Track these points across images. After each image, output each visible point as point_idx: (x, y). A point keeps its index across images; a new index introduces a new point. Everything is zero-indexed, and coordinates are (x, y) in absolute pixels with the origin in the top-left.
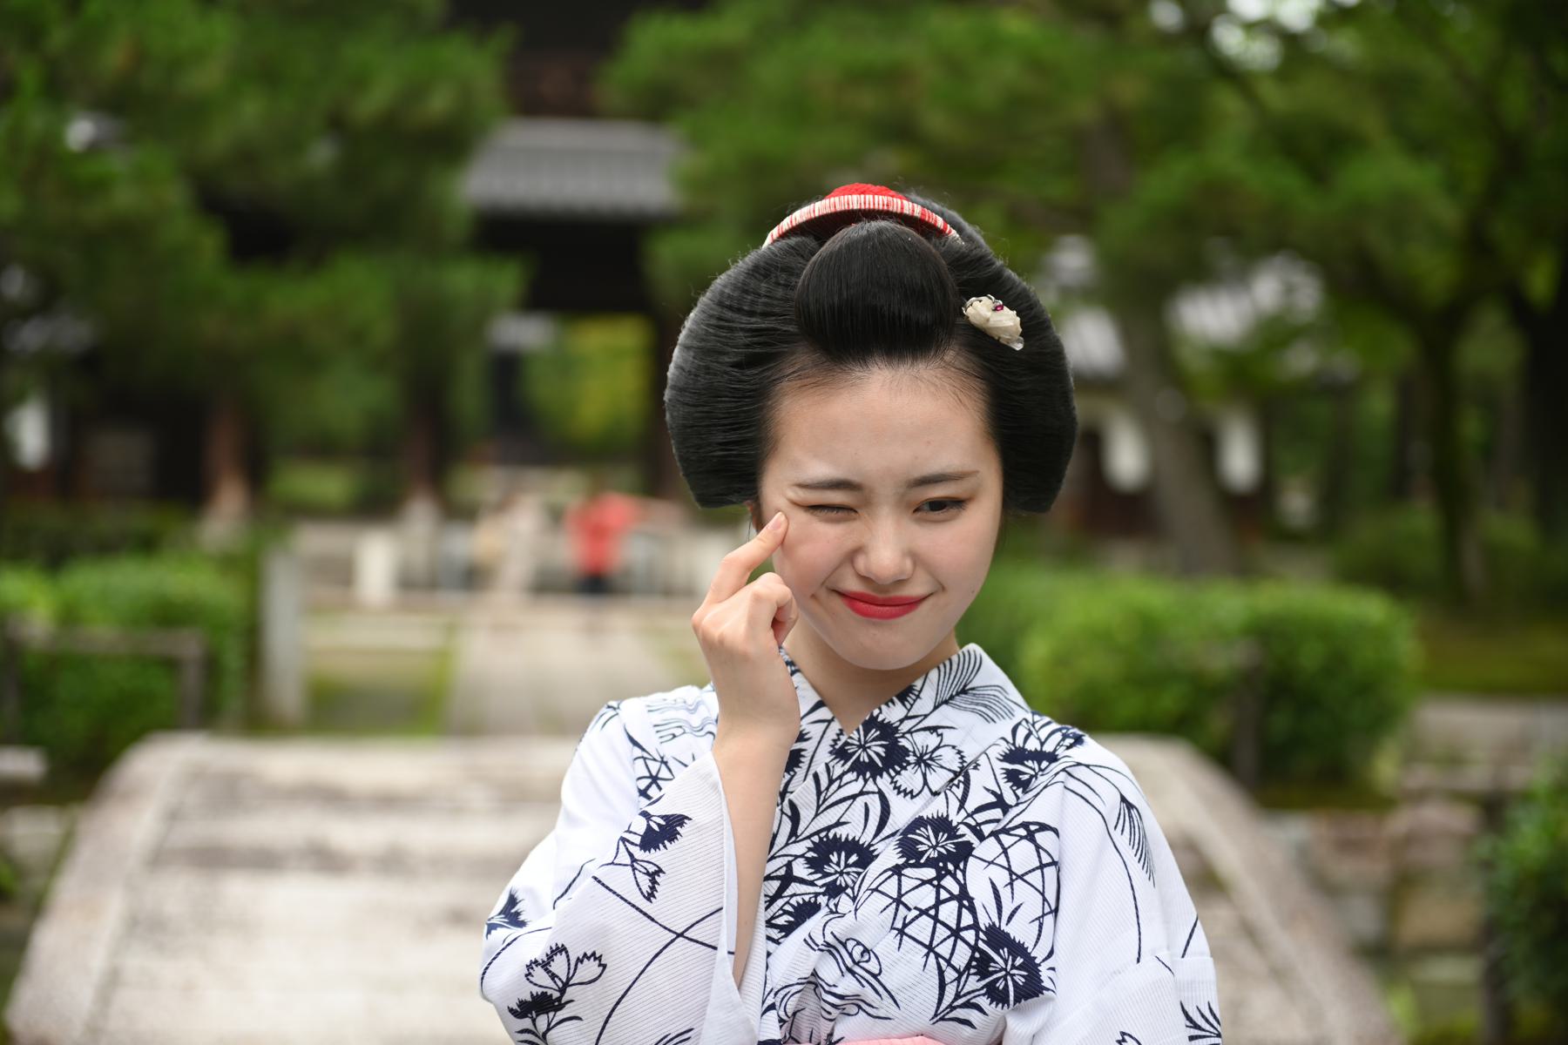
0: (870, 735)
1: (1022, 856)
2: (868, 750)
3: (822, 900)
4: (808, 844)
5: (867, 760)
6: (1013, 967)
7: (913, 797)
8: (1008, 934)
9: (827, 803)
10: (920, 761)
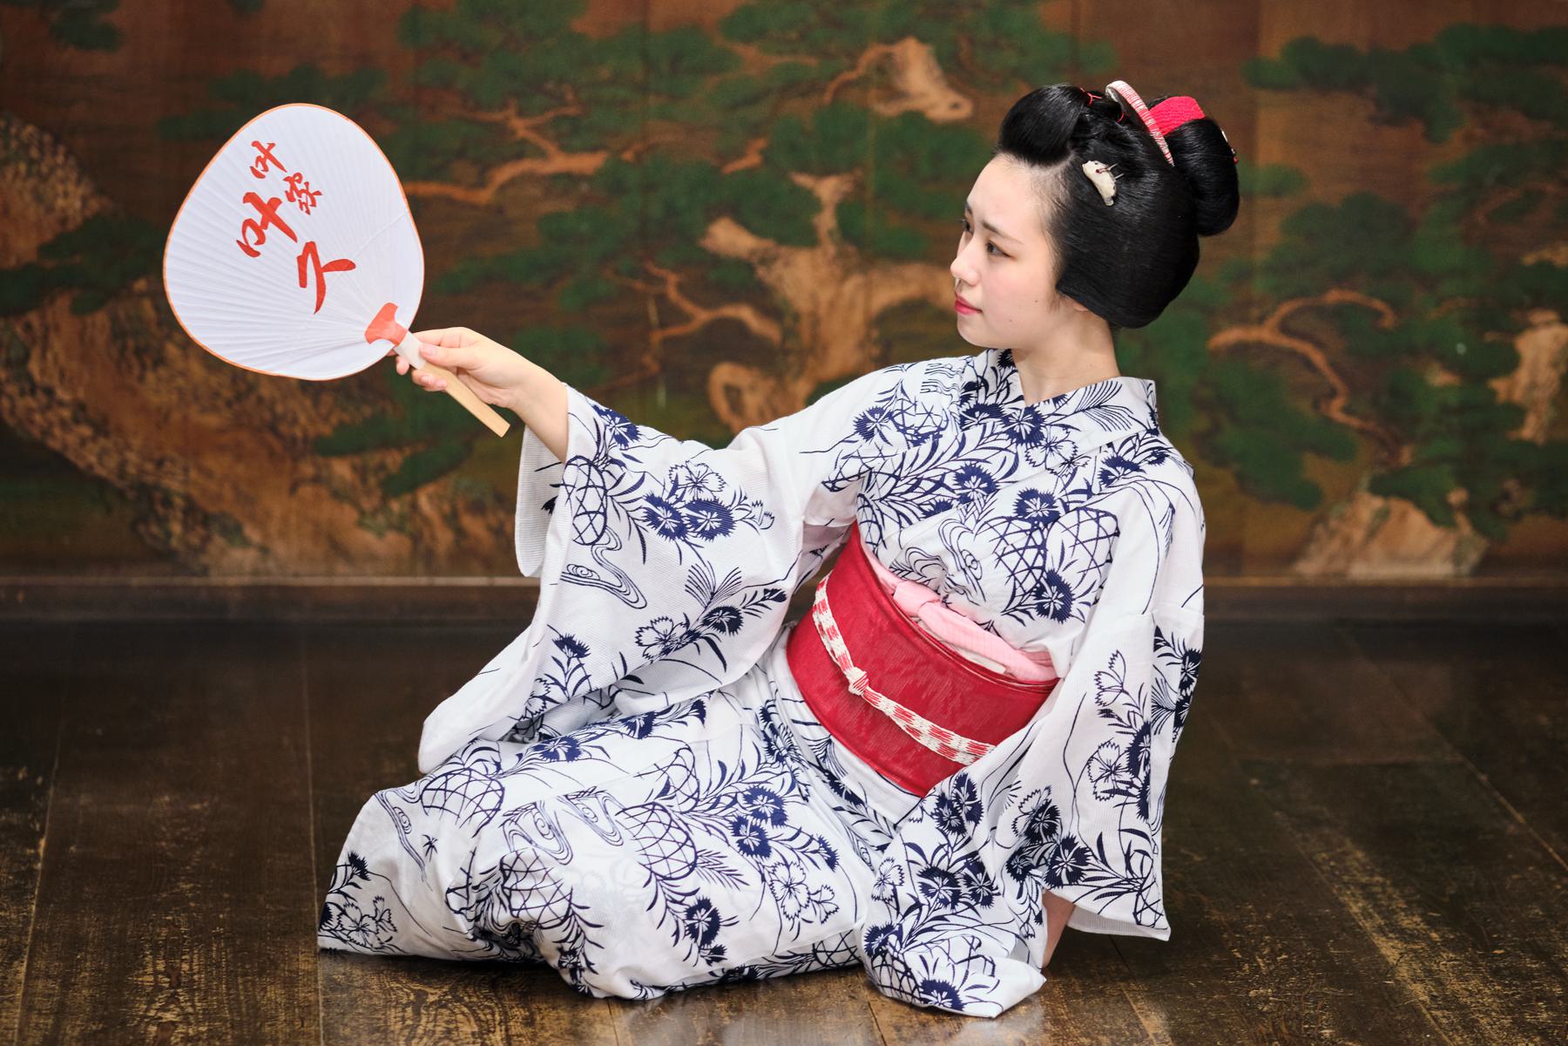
1: (1088, 530)
3: (955, 503)
4: (962, 464)
5: (1018, 431)
6: (1056, 598)
7: (1034, 466)
8: (1061, 578)
9: (984, 446)
10: (1048, 446)
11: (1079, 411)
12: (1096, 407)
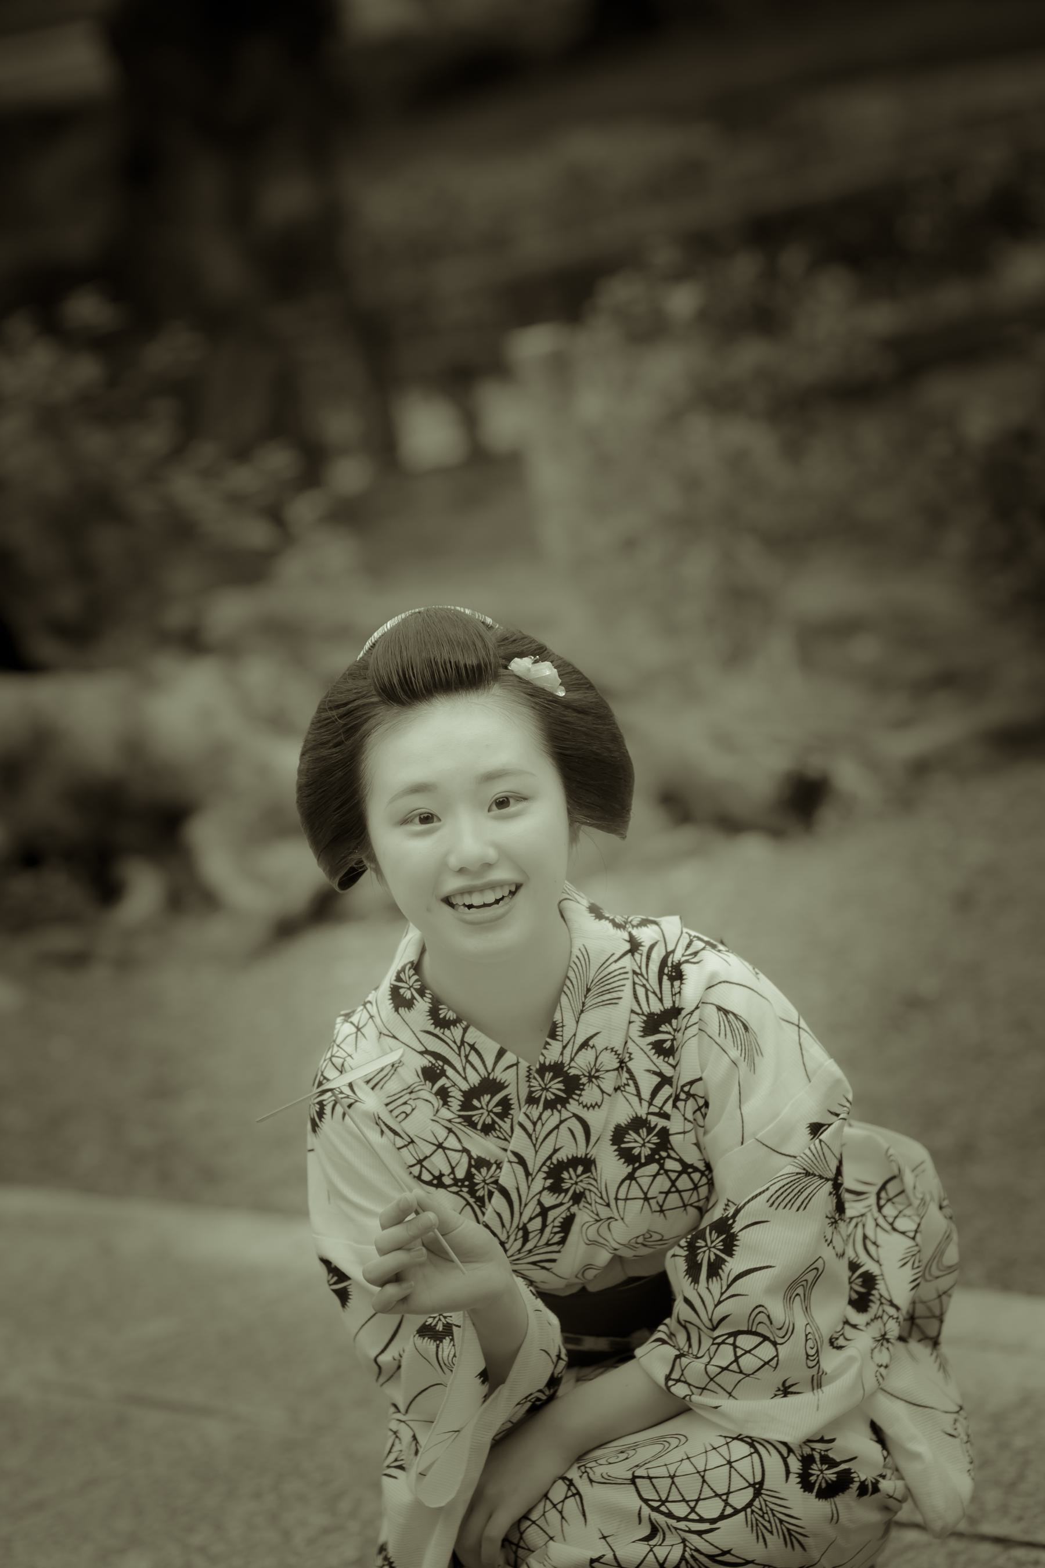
0: (546, 1078)
2: (550, 1090)
3: (574, 1209)
4: (542, 1175)
7: (599, 1107)
9: (540, 1140)
10: (591, 1077)
11: (579, 1018)
12: (587, 993)
